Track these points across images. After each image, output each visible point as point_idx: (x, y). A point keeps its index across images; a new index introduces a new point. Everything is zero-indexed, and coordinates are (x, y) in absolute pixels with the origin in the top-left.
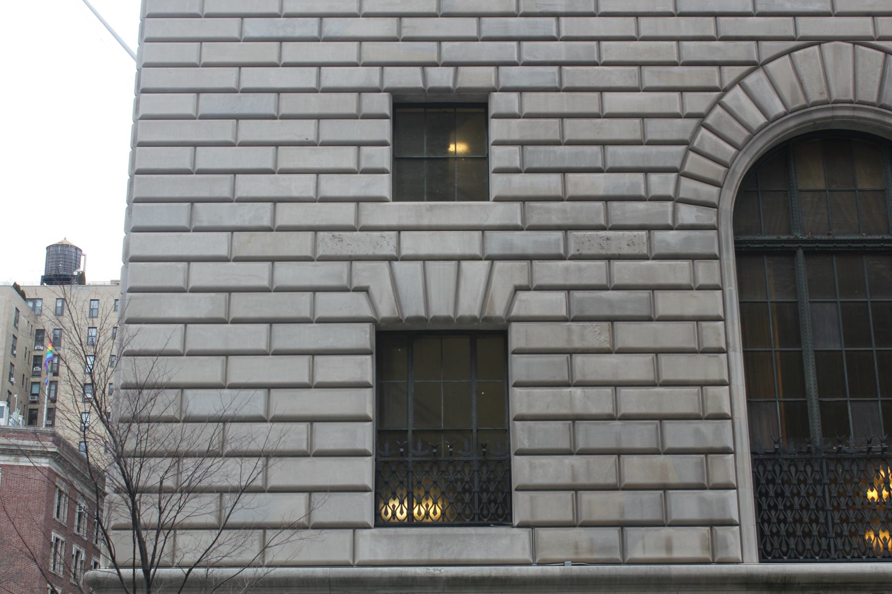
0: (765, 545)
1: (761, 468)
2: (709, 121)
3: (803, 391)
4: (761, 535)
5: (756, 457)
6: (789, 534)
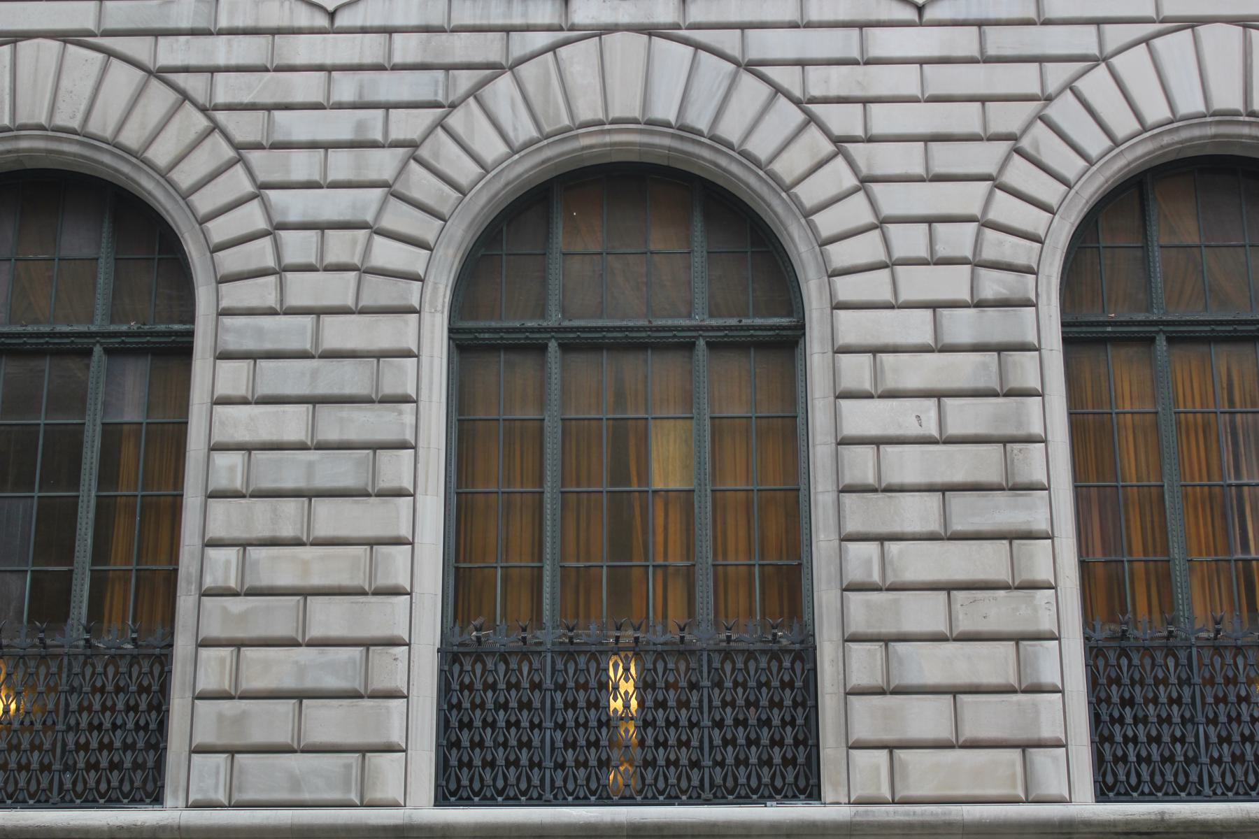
0: (1104, 775)
1: (1101, 663)
2: (424, 152)
3: (67, 554)
4: (1099, 761)
5: (1093, 643)
6: (762, 763)
